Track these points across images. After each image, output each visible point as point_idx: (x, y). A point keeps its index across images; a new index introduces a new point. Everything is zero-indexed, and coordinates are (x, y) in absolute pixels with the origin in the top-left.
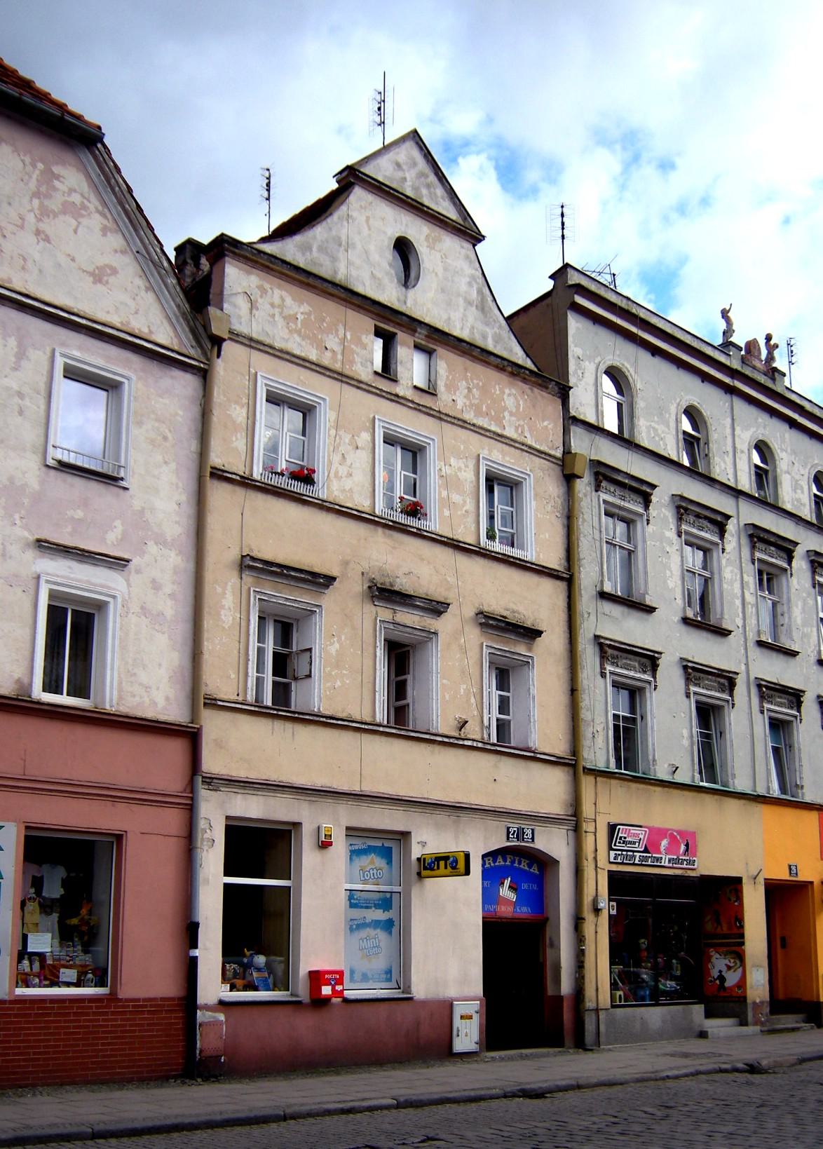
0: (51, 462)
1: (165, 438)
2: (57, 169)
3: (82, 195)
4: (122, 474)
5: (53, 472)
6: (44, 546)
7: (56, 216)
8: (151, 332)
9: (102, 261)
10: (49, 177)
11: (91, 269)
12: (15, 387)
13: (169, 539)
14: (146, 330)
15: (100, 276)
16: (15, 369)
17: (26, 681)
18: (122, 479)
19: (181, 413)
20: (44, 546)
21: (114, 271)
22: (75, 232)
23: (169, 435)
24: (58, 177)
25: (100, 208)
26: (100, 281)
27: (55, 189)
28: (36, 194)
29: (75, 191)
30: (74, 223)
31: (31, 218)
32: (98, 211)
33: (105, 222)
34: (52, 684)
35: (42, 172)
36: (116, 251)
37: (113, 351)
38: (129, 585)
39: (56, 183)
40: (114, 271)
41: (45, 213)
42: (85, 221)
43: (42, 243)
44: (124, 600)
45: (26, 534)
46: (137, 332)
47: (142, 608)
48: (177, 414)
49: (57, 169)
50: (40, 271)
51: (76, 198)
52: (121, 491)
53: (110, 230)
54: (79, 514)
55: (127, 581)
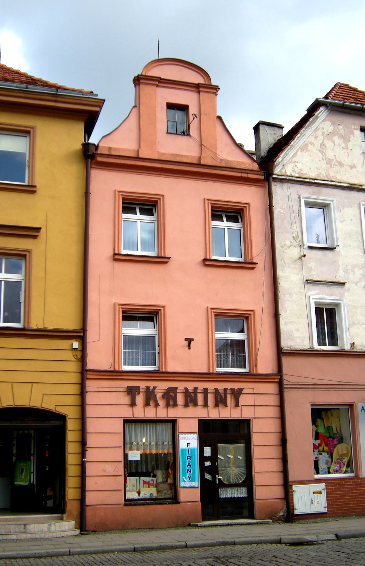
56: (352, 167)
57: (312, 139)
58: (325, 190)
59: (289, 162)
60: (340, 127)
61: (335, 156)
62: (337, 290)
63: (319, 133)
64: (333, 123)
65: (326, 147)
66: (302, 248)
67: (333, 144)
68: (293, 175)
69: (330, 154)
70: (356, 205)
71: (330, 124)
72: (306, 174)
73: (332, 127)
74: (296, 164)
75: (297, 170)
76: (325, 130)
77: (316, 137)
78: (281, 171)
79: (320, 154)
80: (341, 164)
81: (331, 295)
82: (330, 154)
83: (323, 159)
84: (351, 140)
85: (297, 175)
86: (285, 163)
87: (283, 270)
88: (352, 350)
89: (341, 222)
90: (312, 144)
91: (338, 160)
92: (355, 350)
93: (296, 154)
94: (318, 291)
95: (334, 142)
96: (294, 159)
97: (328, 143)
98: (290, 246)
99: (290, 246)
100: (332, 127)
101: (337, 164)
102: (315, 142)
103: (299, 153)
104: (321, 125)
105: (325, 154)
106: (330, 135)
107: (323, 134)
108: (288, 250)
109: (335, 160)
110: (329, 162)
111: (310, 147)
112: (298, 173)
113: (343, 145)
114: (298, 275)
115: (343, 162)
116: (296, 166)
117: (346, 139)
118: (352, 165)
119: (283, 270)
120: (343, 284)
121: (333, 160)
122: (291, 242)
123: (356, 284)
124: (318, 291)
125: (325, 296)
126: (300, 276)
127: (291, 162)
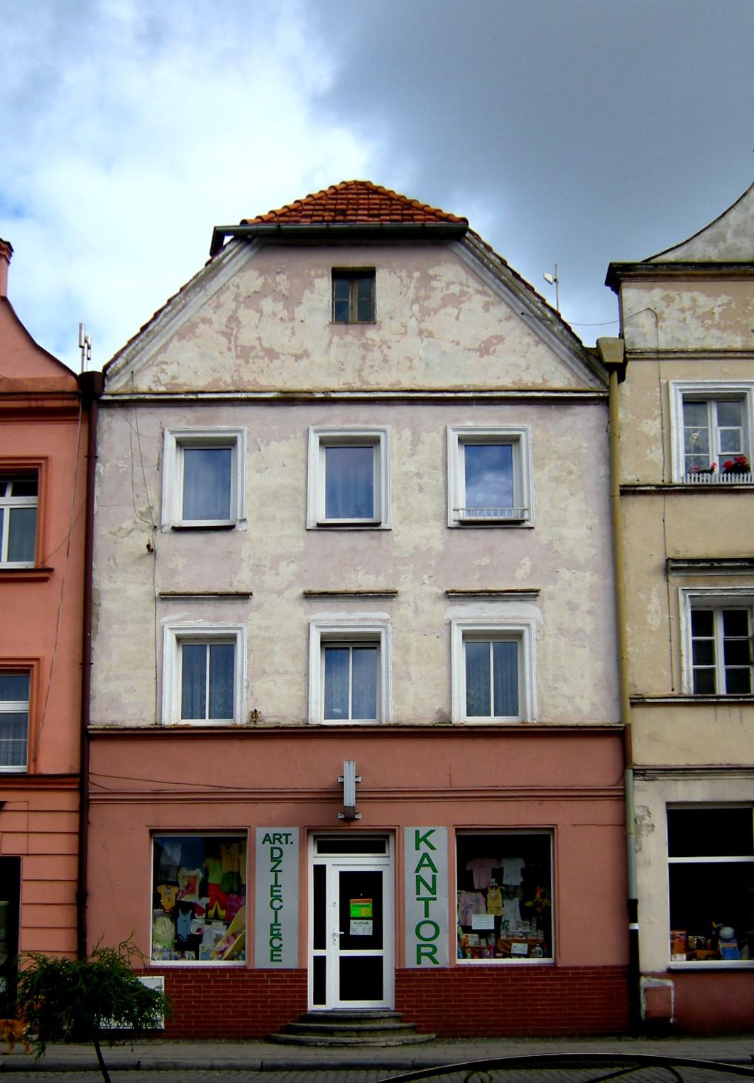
0: (452, 523)
1: (570, 472)
2: (431, 272)
3: (461, 284)
4: (526, 517)
5: (456, 532)
6: (453, 596)
7: (436, 311)
8: (545, 381)
9: (485, 335)
10: (427, 279)
11: (477, 346)
12: (413, 469)
14: (540, 381)
15: (485, 349)
17: (446, 710)
18: (523, 521)
19: (585, 445)
20: (453, 596)
21: (500, 339)
22: (457, 318)
24: (435, 278)
25: (480, 288)
26: (487, 353)
27: (433, 289)
28: (417, 300)
29: (453, 283)
30: (455, 311)
31: (413, 323)
32: (478, 292)
33: (487, 299)
35: (419, 280)
36: (500, 321)
38: (543, 612)
39: (434, 283)
40: (500, 339)
41: (425, 312)
42: (465, 306)
43: (426, 341)
44: (539, 625)
45: (435, 589)
46: (530, 386)
47: (559, 629)
49: (431, 272)
50: (427, 365)
51: (455, 289)
53: (493, 304)
54: (486, 561)
55: (541, 608)
56: (298, 357)
57: (209, 312)
58: (225, 411)
59: (147, 366)
60: (281, 278)
61: (259, 339)
63: (228, 300)
64: (263, 272)
65: (239, 322)
66: (158, 532)
67: (258, 315)
68: (155, 389)
69: (247, 337)
70: (299, 434)
71: (257, 273)
72: (185, 384)
73: (261, 281)
74: (165, 366)
75: (165, 379)
76: (243, 289)
77: (218, 306)
78: (126, 384)
79: (224, 341)
80: (271, 354)
81: (216, 620)
82: (247, 337)
83: (229, 349)
84: (304, 300)
85: (163, 389)
86: (135, 369)
87: (110, 578)
88: (253, 725)
90: (206, 321)
91: (266, 345)
92: (260, 724)
93: (165, 347)
95: (261, 312)
96: (160, 358)
97: (246, 315)
98: (132, 530)
99: (132, 530)
100: (261, 281)
101: (262, 354)
102: (214, 318)
103: (175, 342)
104: (236, 280)
105: (236, 338)
106: (252, 300)
107: (236, 298)
108: (126, 539)
109: (259, 348)
110: (245, 354)
111: (202, 328)
112: (165, 385)
113: (285, 314)
114: (144, 584)
115: (277, 350)
116: (163, 371)
117: (291, 301)
118: (300, 352)
119: (110, 578)
120: (246, 596)
121: (253, 348)
122: (135, 523)
125: (201, 621)
126: (148, 587)
127: (153, 365)
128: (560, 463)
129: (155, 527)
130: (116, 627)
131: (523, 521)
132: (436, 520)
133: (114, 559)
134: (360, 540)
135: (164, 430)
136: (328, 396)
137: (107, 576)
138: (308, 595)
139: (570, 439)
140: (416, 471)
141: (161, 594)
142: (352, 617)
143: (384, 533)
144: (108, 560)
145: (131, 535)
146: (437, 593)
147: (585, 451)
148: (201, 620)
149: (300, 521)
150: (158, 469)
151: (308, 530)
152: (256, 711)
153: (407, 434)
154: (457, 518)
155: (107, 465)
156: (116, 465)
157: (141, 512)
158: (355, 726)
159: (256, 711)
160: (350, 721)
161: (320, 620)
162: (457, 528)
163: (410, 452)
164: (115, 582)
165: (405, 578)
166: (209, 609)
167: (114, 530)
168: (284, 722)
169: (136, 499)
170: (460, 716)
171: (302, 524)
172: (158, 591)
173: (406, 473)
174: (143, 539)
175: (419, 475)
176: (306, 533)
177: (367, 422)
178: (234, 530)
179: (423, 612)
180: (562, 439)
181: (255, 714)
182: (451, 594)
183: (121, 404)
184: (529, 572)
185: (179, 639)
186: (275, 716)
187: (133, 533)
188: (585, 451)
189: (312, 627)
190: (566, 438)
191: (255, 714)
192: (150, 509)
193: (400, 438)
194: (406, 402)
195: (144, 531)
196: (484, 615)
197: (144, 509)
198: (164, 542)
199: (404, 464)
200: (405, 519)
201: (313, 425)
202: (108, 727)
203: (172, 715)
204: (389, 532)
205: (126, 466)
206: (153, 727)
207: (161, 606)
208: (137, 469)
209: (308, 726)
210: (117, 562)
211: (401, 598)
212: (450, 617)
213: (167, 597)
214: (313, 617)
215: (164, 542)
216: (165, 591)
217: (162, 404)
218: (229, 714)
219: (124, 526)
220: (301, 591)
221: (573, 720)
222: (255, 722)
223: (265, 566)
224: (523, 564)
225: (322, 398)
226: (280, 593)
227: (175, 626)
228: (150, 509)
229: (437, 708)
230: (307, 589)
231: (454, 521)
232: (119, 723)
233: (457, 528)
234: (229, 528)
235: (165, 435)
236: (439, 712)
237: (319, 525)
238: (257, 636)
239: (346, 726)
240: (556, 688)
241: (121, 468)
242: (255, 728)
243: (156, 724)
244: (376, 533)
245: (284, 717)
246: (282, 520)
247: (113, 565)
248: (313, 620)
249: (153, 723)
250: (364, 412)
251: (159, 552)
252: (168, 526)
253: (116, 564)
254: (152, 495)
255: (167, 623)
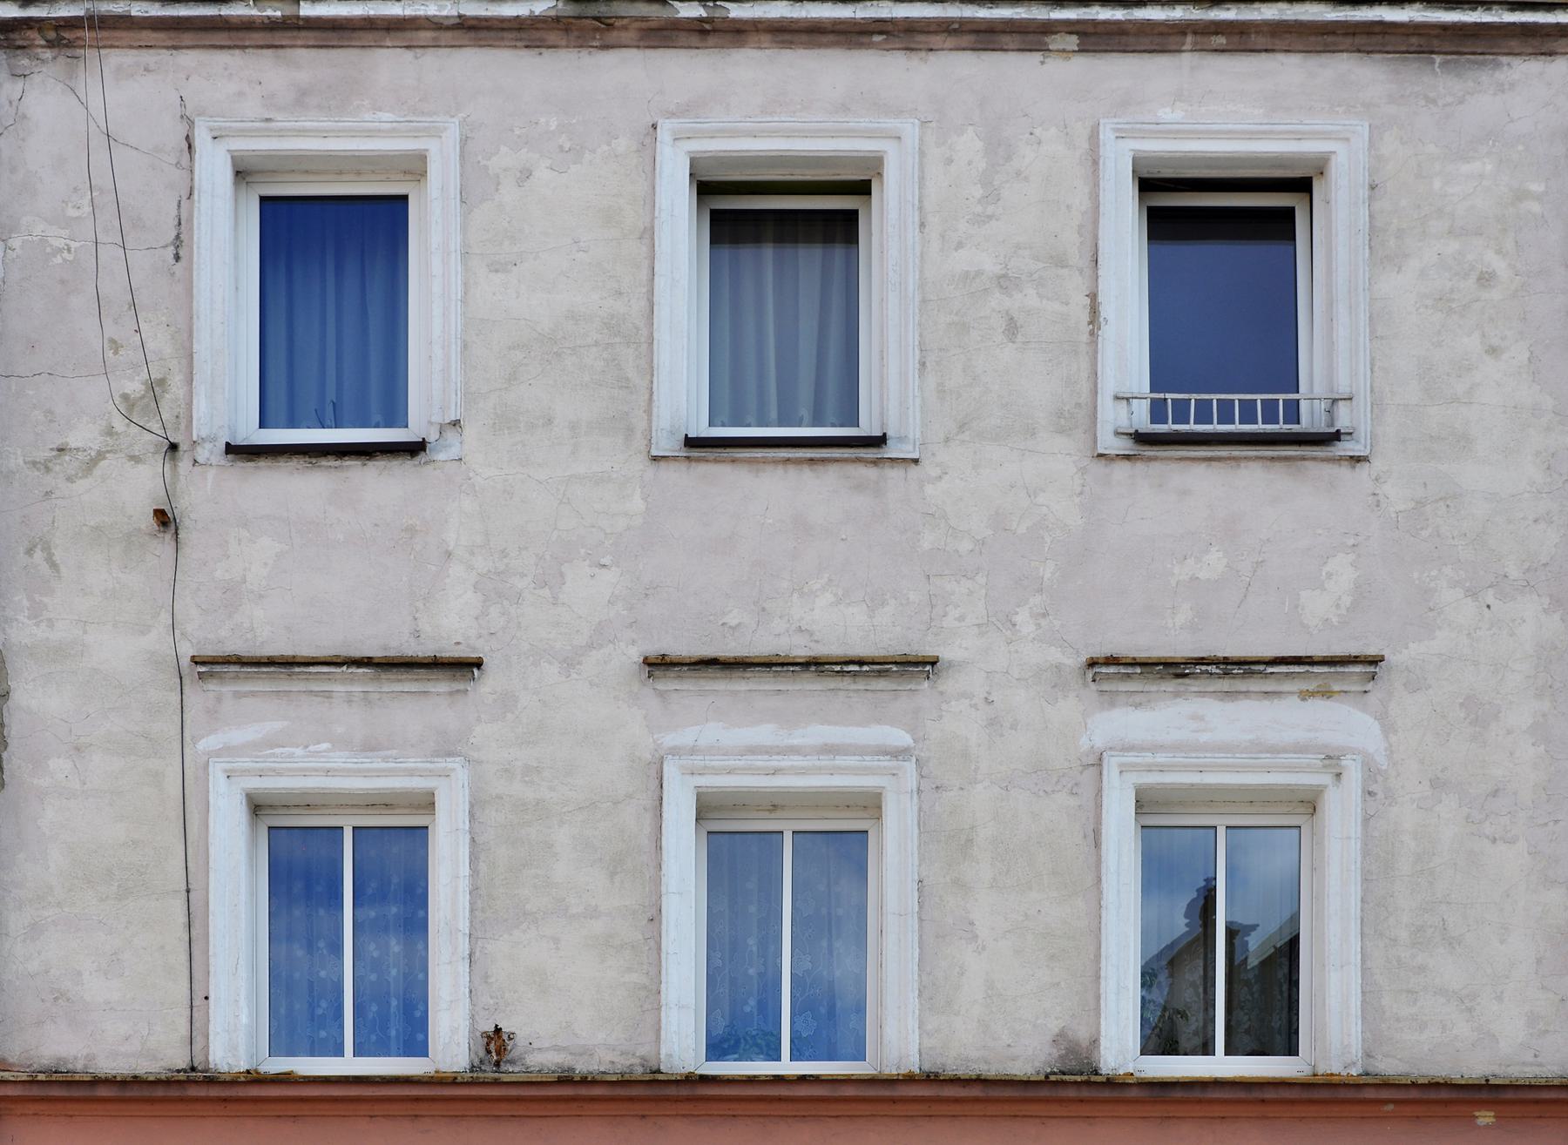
1: (1486, 279)
4: (1342, 423)
5: (1122, 470)
12: (990, 266)
13: (1514, 573)
16: (982, 219)
17: (1082, 1034)
18: (1336, 436)
23: (1499, 265)
34: (1163, 1036)
37: (1288, 71)
38: (1388, 728)
44: (1371, 772)
45: (1055, 655)
47: (1435, 784)
48: (1521, 195)
52: (1344, 471)
54: (1214, 563)
55: (1382, 718)
58: (389, 65)
62: (419, 709)
66: (184, 465)
70: (623, 144)
81: (370, 747)
87: (36, 612)
89: (496, 268)
92: (512, 1072)
94: (278, 725)
98: (101, 455)
99: (101, 455)
108: (81, 485)
114: (144, 630)
119: (36, 612)
120: (467, 666)
122: (110, 432)
123: (570, 663)
124: (278, 725)
126: (156, 639)
128: (1454, 246)
129: (174, 447)
130: (59, 766)
131: (1336, 436)
132: (1061, 431)
133: (47, 549)
134: (818, 491)
135: (191, 124)
136: (718, 14)
137: (26, 603)
138: (658, 665)
139: (1489, 167)
140: (998, 270)
141: (196, 661)
142: (796, 741)
143: (894, 474)
144: (29, 552)
145: (97, 472)
146: (1058, 668)
147: (1535, 207)
148: (325, 746)
149: (630, 431)
150: (177, 258)
151: (655, 459)
152: (498, 1030)
153: (969, 145)
154: (1125, 424)
155: (16, 243)
156: (43, 240)
157: (125, 397)
158: (803, 1079)
159: (498, 1030)
160: (787, 1066)
161: (693, 751)
162: (1127, 457)
163: (979, 209)
164: (51, 623)
165: (961, 618)
166: (347, 705)
167: (43, 454)
168: (582, 1067)
169: (110, 354)
170: (1120, 1049)
171: (639, 442)
172: (187, 651)
173: (966, 276)
174: (139, 485)
175: (1005, 282)
176: (651, 471)
177: (845, 108)
178: (422, 457)
179: (1013, 727)
180: (1465, 168)
181: (496, 1041)
182: (1104, 670)
183: (52, 35)
184: (1347, 601)
185: (257, 807)
186: (558, 1049)
187: (103, 463)
188: (1535, 207)
189: (671, 770)
190: (1475, 167)
191: (496, 1041)
192: (155, 388)
193: (949, 161)
194: (967, 39)
195: (135, 459)
196: (1204, 737)
197: (135, 387)
198: (208, 491)
199: (960, 246)
200: (962, 427)
201: (672, 115)
202: (41, 1077)
203: (237, 1039)
204: (913, 470)
205: (73, 245)
206: (182, 1077)
207: (199, 697)
208: (110, 254)
209: (661, 1077)
210: (57, 558)
211: (949, 684)
212: (1099, 743)
213: (211, 665)
214: (669, 740)
215: (208, 491)
216: (210, 651)
217: (187, 38)
218: (416, 1044)
219: (74, 441)
220: (635, 654)
221: (1475, 1066)
222: (497, 1064)
223: (523, 575)
224: (1329, 575)
225: (701, 20)
226: (570, 663)
227: (245, 763)
228: (155, 388)
229: (1054, 1026)
230: (654, 648)
231: (1117, 433)
232: (79, 1066)
233: (1127, 457)
234: (414, 449)
235: (197, 143)
236: (1060, 1038)
237: (692, 443)
238: (499, 797)
239: (778, 1080)
240: (1422, 969)
241: (60, 250)
242: (497, 1083)
243: (193, 1069)
244: (871, 473)
245: (587, 1052)
246: (574, 427)
247: (45, 568)
248: (675, 751)
249: (182, 1062)
250: (834, 71)
251: (186, 524)
252: (213, 440)
253: (54, 566)
254: (159, 341)
255: (218, 753)
